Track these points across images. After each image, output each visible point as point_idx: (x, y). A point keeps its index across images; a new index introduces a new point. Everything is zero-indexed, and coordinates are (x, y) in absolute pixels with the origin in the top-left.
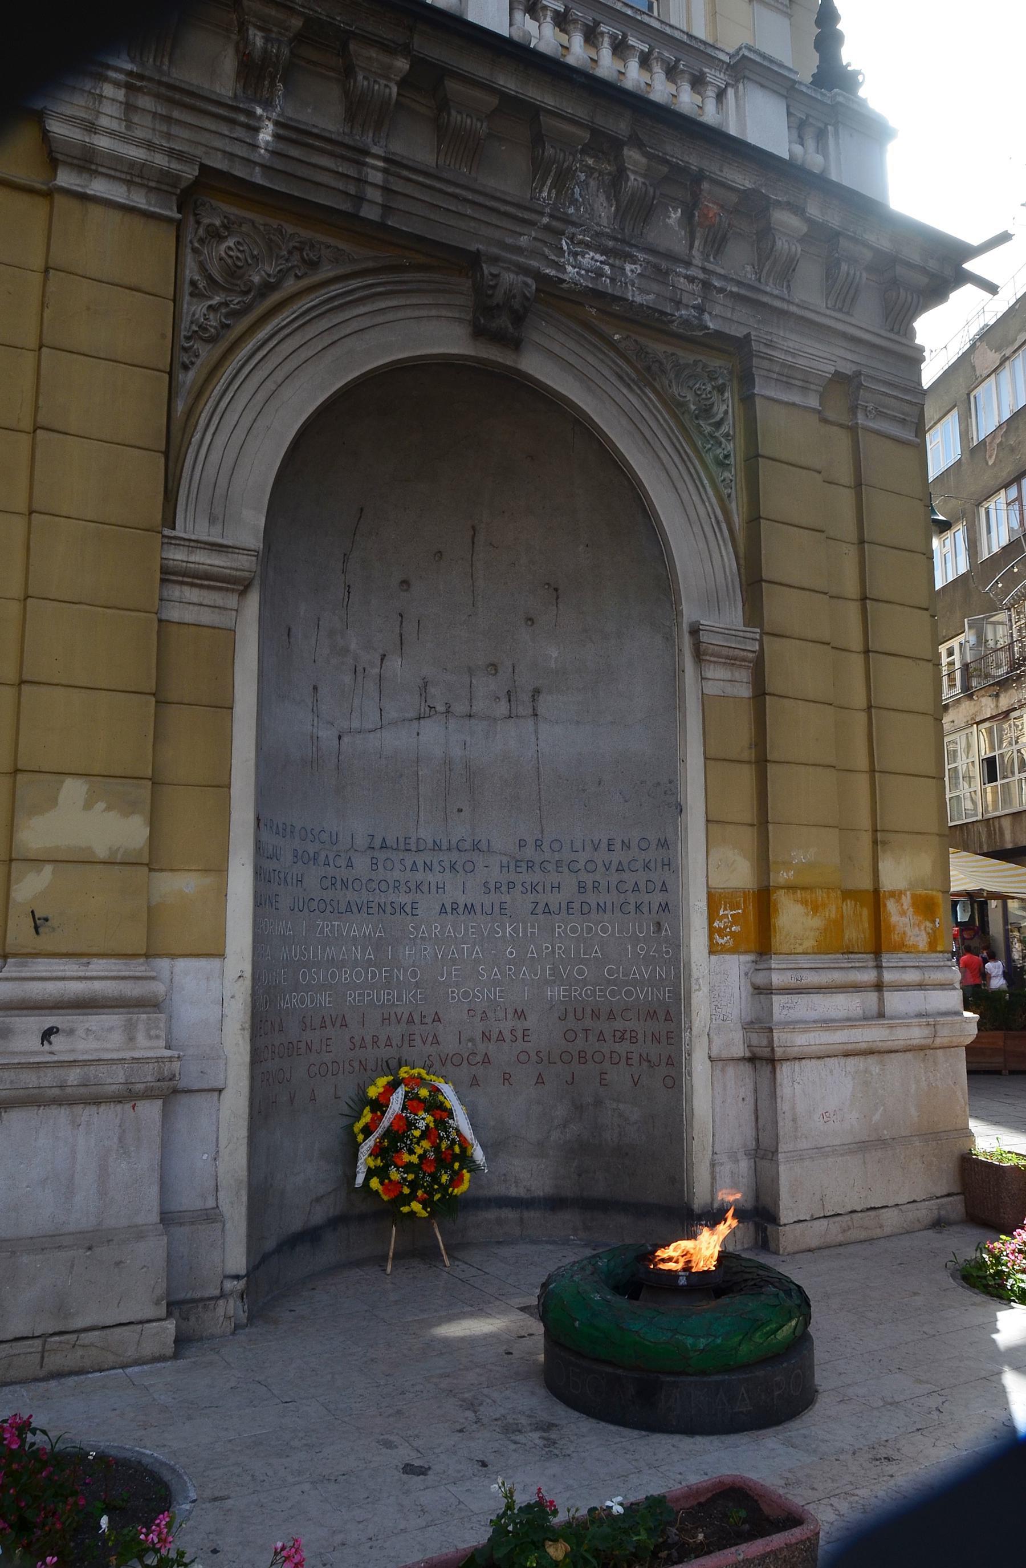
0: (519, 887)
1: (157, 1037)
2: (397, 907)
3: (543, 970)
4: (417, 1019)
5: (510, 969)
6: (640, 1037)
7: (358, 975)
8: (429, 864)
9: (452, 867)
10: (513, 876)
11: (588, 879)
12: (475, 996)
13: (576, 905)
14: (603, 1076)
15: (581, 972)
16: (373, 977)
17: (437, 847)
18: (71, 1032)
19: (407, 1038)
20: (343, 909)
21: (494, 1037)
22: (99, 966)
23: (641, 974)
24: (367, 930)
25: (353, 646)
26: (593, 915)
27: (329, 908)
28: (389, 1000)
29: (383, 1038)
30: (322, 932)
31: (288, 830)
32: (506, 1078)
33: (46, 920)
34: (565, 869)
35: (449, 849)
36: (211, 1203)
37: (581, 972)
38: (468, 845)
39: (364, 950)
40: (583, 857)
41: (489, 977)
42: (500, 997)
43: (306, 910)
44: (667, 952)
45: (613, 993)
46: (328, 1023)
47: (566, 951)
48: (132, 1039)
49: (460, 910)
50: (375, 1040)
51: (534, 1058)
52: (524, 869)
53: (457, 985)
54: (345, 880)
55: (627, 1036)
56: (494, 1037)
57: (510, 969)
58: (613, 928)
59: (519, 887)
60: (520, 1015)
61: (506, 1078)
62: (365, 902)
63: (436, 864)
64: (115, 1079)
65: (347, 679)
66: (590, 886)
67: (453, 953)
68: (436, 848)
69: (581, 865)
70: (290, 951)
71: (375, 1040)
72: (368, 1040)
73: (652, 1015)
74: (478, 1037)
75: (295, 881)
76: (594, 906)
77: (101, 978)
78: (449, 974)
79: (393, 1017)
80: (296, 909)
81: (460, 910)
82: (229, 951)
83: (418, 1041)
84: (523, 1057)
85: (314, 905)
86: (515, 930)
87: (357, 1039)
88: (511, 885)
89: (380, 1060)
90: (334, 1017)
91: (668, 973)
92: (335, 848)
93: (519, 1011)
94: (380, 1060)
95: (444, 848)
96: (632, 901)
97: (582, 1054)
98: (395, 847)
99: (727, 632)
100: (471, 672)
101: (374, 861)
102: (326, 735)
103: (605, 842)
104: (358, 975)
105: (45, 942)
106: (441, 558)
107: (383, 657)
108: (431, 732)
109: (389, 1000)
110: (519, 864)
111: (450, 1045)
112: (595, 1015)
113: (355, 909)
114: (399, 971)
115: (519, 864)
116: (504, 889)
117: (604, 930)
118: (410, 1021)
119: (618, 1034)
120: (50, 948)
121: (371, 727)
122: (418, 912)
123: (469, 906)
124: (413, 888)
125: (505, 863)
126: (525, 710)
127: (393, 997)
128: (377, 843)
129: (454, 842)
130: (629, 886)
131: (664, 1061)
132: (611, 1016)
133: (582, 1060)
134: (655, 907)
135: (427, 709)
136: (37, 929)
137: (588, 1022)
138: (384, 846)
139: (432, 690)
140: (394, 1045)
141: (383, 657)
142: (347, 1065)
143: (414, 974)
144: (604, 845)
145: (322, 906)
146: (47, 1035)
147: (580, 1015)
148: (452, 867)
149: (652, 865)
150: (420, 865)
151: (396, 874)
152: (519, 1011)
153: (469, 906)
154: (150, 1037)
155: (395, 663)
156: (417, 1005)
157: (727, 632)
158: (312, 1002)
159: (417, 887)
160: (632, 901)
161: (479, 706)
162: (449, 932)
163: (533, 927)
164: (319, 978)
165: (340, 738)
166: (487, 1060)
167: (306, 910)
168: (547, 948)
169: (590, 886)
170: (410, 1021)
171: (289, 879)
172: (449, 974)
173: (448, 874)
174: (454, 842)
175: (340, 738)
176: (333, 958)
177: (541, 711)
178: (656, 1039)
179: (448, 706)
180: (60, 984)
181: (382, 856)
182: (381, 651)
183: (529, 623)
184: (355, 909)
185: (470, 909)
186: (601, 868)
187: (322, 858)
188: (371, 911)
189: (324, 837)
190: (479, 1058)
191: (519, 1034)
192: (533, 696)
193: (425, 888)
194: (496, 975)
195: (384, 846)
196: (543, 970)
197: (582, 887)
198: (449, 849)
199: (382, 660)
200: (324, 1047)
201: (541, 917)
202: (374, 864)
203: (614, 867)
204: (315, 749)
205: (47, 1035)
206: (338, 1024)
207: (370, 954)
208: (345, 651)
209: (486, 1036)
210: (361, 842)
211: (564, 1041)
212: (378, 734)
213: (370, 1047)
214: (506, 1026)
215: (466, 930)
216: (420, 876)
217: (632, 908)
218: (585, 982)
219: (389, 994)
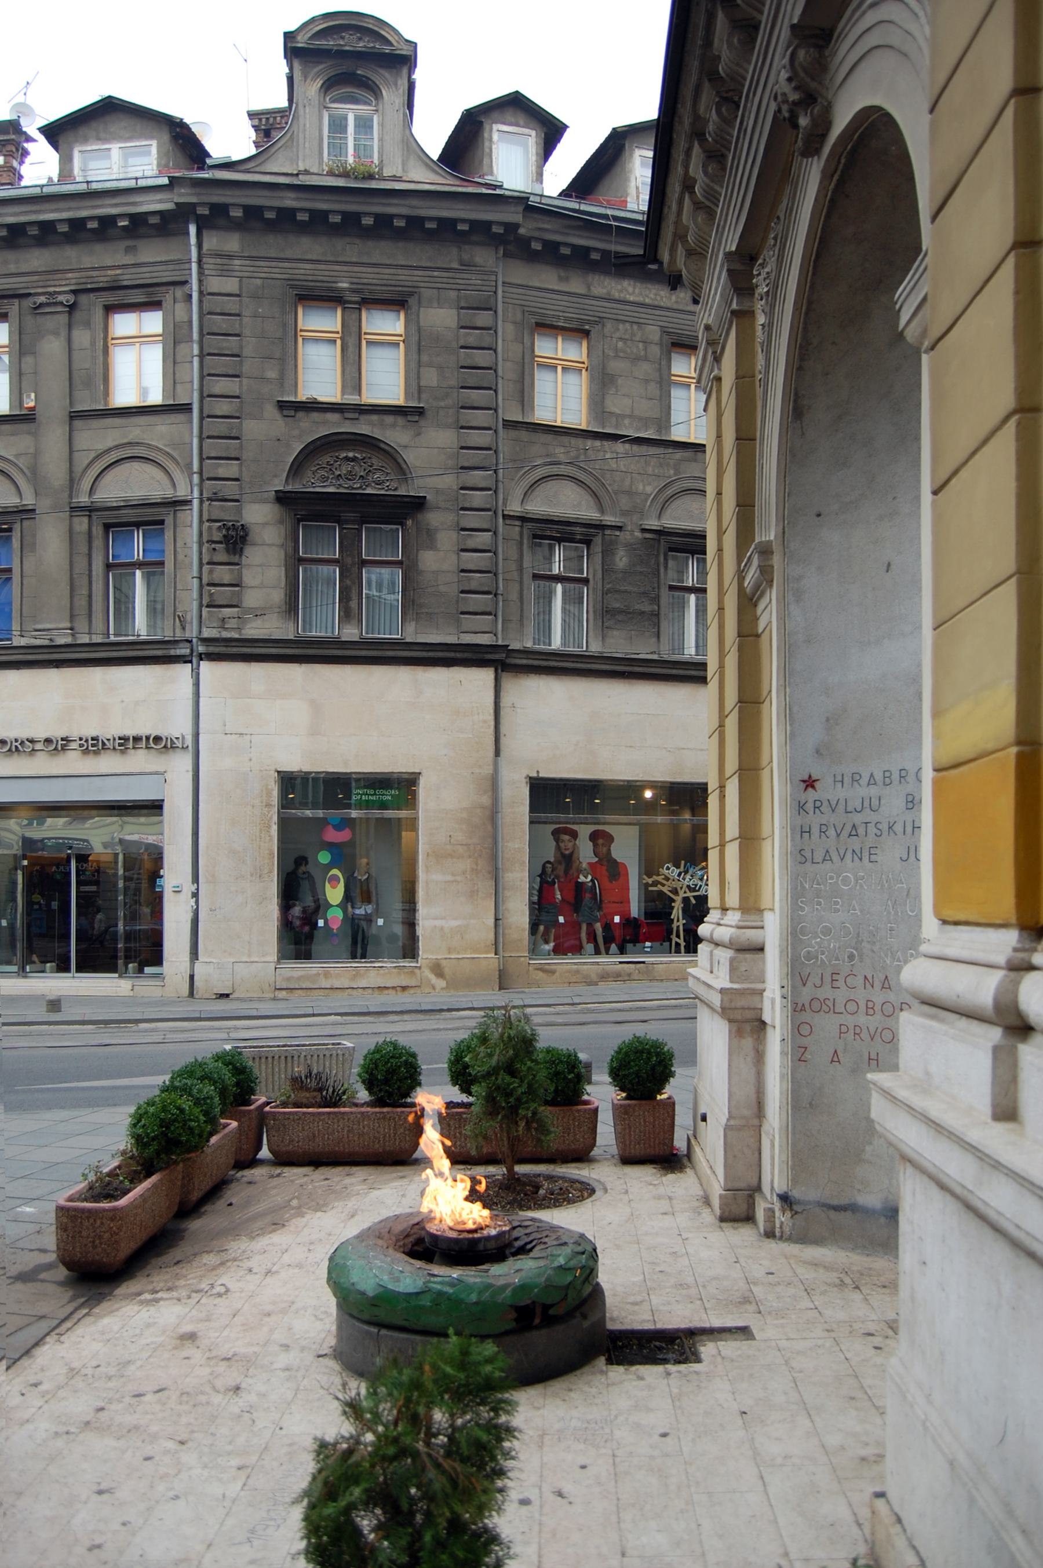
171: (898, 828)
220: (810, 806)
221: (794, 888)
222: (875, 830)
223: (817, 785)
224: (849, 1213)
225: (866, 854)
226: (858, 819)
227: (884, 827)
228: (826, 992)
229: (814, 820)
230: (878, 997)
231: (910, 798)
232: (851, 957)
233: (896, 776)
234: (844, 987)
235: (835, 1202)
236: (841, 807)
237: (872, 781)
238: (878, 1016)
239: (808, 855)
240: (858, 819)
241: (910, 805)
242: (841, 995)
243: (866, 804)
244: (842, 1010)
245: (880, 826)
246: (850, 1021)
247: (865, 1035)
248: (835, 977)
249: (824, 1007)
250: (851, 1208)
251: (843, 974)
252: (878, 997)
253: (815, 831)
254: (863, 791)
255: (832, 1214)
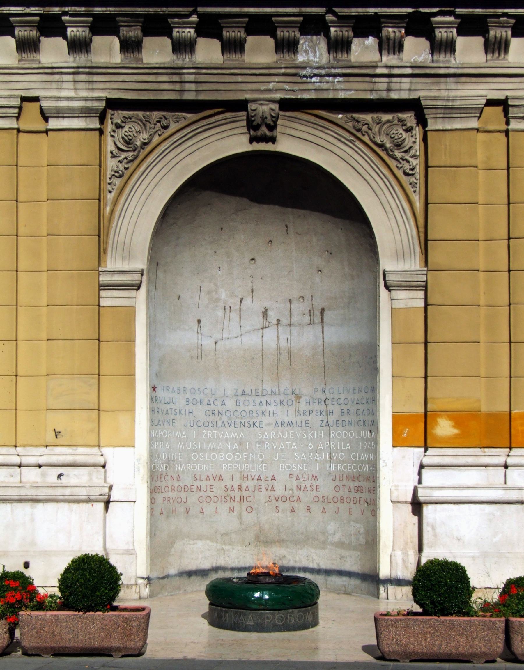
0: (314, 413)
1: (101, 478)
2: (251, 423)
3: (326, 455)
4: (263, 478)
5: (310, 455)
6: (364, 490)
7: (229, 456)
8: (269, 402)
9: (282, 403)
10: (312, 407)
11: (345, 408)
12: (293, 468)
13: (340, 422)
14: (351, 510)
15: (342, 457)
16: (238, 457)
17: (273, 393)
18: (68, 476)
19: (257, 487)
20: (220, 424)
21: (302, 489)
22: (80, 450)
23: (365, 459)
24: (234, 435)
25: (223, 296)
26: (347, 427)
27: (211, 425)
28: (247, 469)
29: (244, 487)
30: (206, 436)
31: (182, 389)
32: (308, 509)
33: (60, 432)
34: (335, 403)
35: (279, 394)
36: (131, 547)
37: (342, 457)
38: (289, 392)
39: (232, 445)
40: (343, 397)
41: (300, 458)
42: (305, 468)
43: (195, 426)
44: (373, 447)
45: (355, 467)
46: (211, 478)
47: (336, 446)
48: (91, 479)
49: (286, 425)
50: (240, 488)
51: (321, 500)
52: (316, 403)
53: (284, 462)
54: (221, 412)
55: (359, 489)
56: (302, 489)
57: (310, 455)
58: (355, 433)
59: (314, 413)
60: (315, 478)
61: (308, 509)
62: (233, 421)
63: (272, 401)
64: (83, 494)
65: (220, 313)
66: (346, 412)
67: (282, 446)
68: (273, 394)
69: (341, 401)
70: (185, 445)
71: (240, 488)
72: (236, 487)
73: (368, 479)
74: (295, 488)
75: (187, 413)
76: (347, 422)
77: (82, 454)
78: (280, 456)
79: (249, 477)
80: (189, 425)
81: (286, 425)
82: (136, 445)
83: (263, 489)
84: (316, 499)
85: (200, 424)
86: (313, 434)
87: (229, 487)
88: (311, 412)
89: (242, 497)
90: (215, 476)
91: (374, 458)
92: (214, 396)
93: (314, 476)
94: (242, 497)
95: (277, 393)
96: (362, 420)
97: (342, 498)
98: (250, 394)
99: (404, 273)
100: (290, 301)
101: (238, 402)
102: (207, 343)
103: (352, 388)
104: (229, 456)
105: (60, 441)
106: (272, 244)
107: (242, 300)
108: (270, 334)
109: (247, 469)
110: (315, 401)
111: (279, 491)
112: (348, 478)
113: (227, 425)
114: (253, 455)
115: (315, 401)
116: (307, 413)
117: (351, 434)
118: (259, 479)
119: (356, 488)
120: (62, 444)
121: (236, 335)
122: (263, 426)
123: (290, 423)
124: (260, 414)
125: (308, 401)
126: (318, 319)
127: (250, 468)
128: (240, 392)
129: (282, 390)
130: (360, 412)
131: (372, 502)
132: (354, 480)
133: (342, 501)
134: (370, 423)
135: (267, 323)
136: (56, 436)
137: (344, 482)
138: (244, 393)
139: (270, 313)
140: (250, 490)
141: (242, 300)
142: (223, 498)
143: (261, 456)
144: (351, 391)
145: (206, 424)
146: (60, 476)
147: (341, 479)
148: (282, 403)
149: (369, 401)
150: (264, 403)
151: (251, 408)
152: (314, 476)
153: (290, 423)
154: (97, 478)
155: (248, 302)
156: (262, 472)
157: (404, 273)
158: (200, 468)
159: (263, 413)
160: (362, 420)
161: (295, 319)
162: (280, 436)
163: (321, 433)
164: (205, 457)
165: (216, 343)
166: (299, 500)
167: (195, 426)
168: (327, 444)
169: (346, 412)
170: (259, 479)
172: (280, 456)
173: (279, 406)
174: (282, 390)
175: (216, 343)
176: (213, 448)
177: (325, 319)
178: (369, 491)
179: (278, 321)
180: (64, 457)
181: (242, 399)
182: (241, 297)
183: (320, 272)
184: (227, 425)
185: (290, 424)
186: (350, 402)
187: (206, 401)
188: (236, 426)
189: (206, 391)
190: (295, 498)
191: (314, 488)
192: (321, 312)
193: (267, 414)
194: (303, 457)
195: (244, 393)
196: (326, 455)
197: (342, 413)
198: (279, 394)
199: (241, 301)
200: (209, 489)
201: (325, 428)
202: (238, 403)
203: (355, 402)
204: (199, 350)
205: (60, 476)
206: (217, 478)
207: (236, 447)
208: (218, 300)
209: (298, 488)
210: (229, 392)
211: (334, 491)
212: (239, 339)
213: (236, 490)
214: (308, 484)
215: (289, 434)
216: (264, 408)
217: (361, 423)
218: (343, 462)
219: (247, 466)
220: (154, 399)
221: (150, 436)
222: (174, 413)
223: (156, 389)
224: (166, 579)
225: (171, 423)
226: (168, 407)
227: (178, 411)
228: (158, 484)
229: (155, 405)
230: (176, 484)
231: (188, 400)
232: (166, 468)
233: (182, 389)
234: (164, 481)
235: (161, 576)
236: (163, 402)
237: (173, 391)
238: (176, 492)
239: (154, 421)
240: (168, 407)
241: (188, 403)
242: (163, 484)
243: (171, 401)
244: (163, 491)
245: (176, 411)
246: (166, 495)
247: (171, 501)
248: (162, 476)
249: (158, 490)
250: (167, 577)
251: (164, 475)
252: (176, 484)
253: (156, 410)
254: (171, 395)
255: (161, 581)
